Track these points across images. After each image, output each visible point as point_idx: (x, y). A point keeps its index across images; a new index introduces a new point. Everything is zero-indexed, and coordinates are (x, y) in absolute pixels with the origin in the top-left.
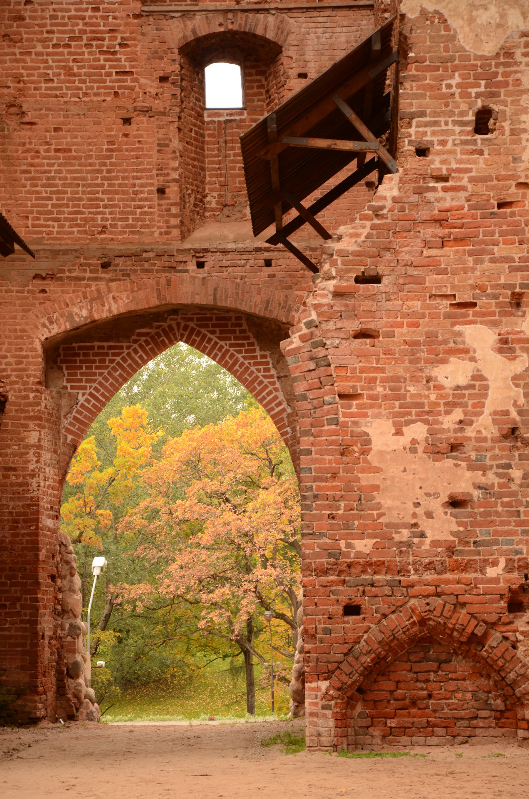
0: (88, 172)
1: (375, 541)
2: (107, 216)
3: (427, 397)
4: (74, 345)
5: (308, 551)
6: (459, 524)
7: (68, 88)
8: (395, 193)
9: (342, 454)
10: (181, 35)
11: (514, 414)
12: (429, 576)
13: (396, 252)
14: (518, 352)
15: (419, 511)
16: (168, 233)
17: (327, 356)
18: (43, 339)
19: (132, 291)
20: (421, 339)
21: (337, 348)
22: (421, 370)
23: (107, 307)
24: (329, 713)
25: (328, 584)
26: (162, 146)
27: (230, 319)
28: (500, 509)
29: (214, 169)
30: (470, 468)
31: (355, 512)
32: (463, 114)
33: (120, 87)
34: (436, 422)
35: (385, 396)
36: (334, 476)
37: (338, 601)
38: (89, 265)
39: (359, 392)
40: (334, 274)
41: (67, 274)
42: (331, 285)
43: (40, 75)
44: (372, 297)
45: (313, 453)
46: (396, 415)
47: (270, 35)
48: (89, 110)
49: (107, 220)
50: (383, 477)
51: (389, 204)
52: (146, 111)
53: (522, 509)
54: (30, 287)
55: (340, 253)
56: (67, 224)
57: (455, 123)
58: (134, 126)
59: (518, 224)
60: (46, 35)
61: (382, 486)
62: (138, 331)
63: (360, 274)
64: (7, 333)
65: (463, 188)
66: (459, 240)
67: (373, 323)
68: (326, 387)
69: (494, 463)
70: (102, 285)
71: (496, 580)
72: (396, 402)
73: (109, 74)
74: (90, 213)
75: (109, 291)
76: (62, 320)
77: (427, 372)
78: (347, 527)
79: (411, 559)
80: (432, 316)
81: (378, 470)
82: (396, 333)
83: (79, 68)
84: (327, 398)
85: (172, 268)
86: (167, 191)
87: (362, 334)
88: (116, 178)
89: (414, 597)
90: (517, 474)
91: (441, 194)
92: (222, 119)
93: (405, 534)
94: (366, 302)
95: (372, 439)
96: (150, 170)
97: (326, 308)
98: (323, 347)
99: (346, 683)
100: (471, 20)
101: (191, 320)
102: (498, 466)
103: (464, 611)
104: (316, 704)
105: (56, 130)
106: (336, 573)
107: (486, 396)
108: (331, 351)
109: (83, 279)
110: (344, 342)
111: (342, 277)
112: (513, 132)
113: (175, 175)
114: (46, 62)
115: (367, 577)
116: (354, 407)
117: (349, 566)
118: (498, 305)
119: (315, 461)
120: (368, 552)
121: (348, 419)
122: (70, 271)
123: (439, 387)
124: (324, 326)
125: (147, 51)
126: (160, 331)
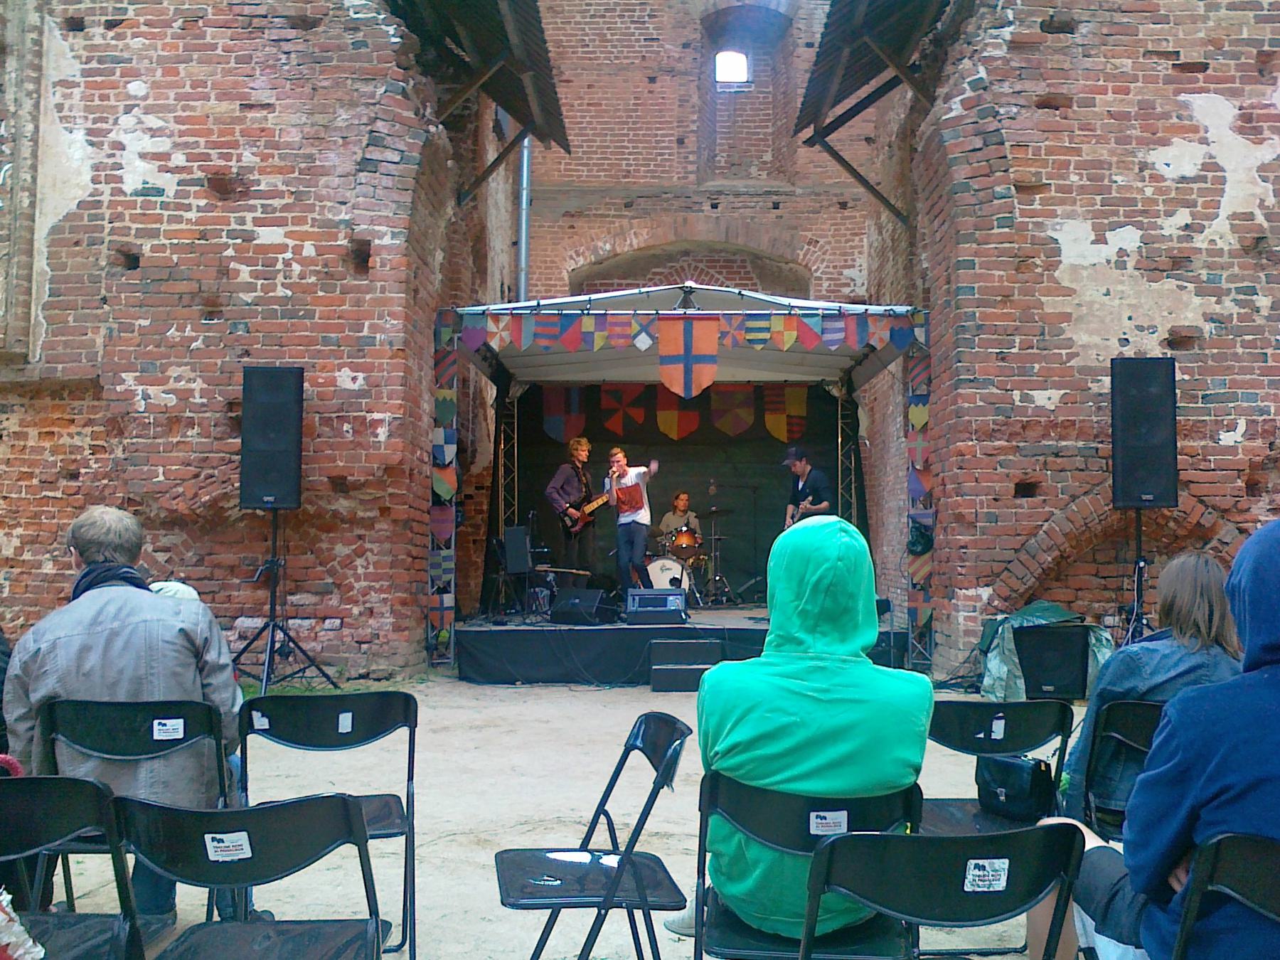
0: (616, 123)
1: (1062, 392)
2: (631, 162)
3: (1141, 191)
4: (598, 282)
5: (966, 405)
7: (601, 52)
10: (703, 8)
11: (1260, 219)
14: (1267, 133)
16: (686, 178)
17: (998, 130)
18: (570, 269)
19: (652, 228)
20: (1133, 110)
21: (1014, 119)
22: (1133, 154)
23: (628, 242)
25: (995, 452)
26: (683, 101)
27: (735, 261)
28: (1240, 350)
29: (725, 133)
31: (1035, 351)
33: (647, 52)
35: (1082, 187)
36: (1007, 297)
37: (1008, 476)
38: (614, 204)
39: (1045, 181)
40: (1011, 17)
41: (594, 212)
42: (1007, 32)
43: (578, 41)
44: (1063, 51)
45: (977, 266)
46: (1096, 215)
48: (619, 70)
49: (631, 165)
50: (1077, 302)
52: (671, 72)
53: (1269, 351)
54: (560, 223)
56: (595, 168)
58: (658, 84)
60: (584, 7)
61: (1074, 316)
62: (654, 270)
63: (1048, 18)
64: (539, 264)
67: (1065, 86)
68: (998, 174)
69: (1232, 286)
70: (625, 222)
71: (1232, 450)
72: (1096, 197)
73: (637, 41)
74: (616, 159)
75: (631, 228)
76: (587, 254)
80: (1147, 79)
81: (1070, 292)
82: (1097, 100)
83: (612, 35)
84: (998, 189)
86: (686, 141)
87: (1046, 103)
88: (640, 129)
90: (1263, 302)
92: (732, 90)
94: (1056, 57)
95: (1063, 248)
96: (670, 122)
97: (999, 62)
98: (994, 117)
99: (1016, 591)
101: (701, 261)
102: (1239, 290)
104: (973, 619)
105: (589, 87)
106: (1006, 437)
108: (1006, 123)
109: (608, 216)
110: (1023, 111)
111: (1022, 22)
114: (583, 29)
115: (1050, 443)
116: (1038, 202)
118: (1239, 67)
119: (980, 277)
120: (1053, 408)
121: (1028, 220)
122: (596, 209)
124: (996, 88)
125: (673, 21)
126: (673, 271)
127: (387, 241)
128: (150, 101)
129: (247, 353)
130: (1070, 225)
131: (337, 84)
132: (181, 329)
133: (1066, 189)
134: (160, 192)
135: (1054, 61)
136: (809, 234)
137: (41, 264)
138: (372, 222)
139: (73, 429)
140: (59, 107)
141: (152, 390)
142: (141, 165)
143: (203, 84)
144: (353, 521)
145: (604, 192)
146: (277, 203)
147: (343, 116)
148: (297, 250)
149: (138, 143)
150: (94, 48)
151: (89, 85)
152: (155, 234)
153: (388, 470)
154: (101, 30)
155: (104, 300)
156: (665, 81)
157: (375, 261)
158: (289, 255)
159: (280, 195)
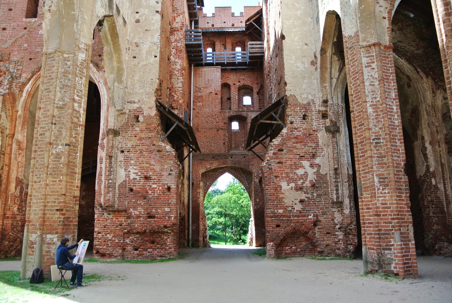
3: (294, 177)
6: (302, 206)
8: (286, 132)
9: (275, 190)
11: (314, 181)
12: (295, 218)
13: (287, 145)
14: (315, 167)
15: (293, 203)
20: (293, 164)
22: (293, 171)
24: (273, 250)
26: (224, 135)
28: (311, 203)
30: (305, 193)
32: (300, 115)
34: (297, 183)
36: (274, 194)
42: (272, 151)
44: (282, 154)
46: (287, 181)
47: (245, 116)
51: (285, 134)
52: (222, 129)
53: (316, 203)
55: (274, 144)
57: (298, 117)
59: (313, 139)
65: (301, 131)
66: (300, 142)
70: (213, 161)
71: (311, 219)
77: (294, 171)
78: (277, 207)
79: (292, 214)
80: (295, 159)
81: (284, 194)
84: (272, 177)
85: (226, 158)
87: (279, 163)
90: (315, 195)
91: (296, 132)
93: (290, 208)
100: (301, 97)
102: (311, 193)
107: (308, 177)
108: (273, 166)
112: (311, 120)
117: (277, 216)
118: (310, 156)
119: (269, 191)
123: (297, 175)
124: (271, 161)
127: (173, 187)
128: (135, 164)
129: (151, 205)
130: (283, 183)
131: (165, 161)
132: (140, 201)
133: (283, 177)
134: (136, 179)
135: (280, 156)
136: (252, 163)
137: (117, 191)
138: (171, 184)
139: (121, 218)
140: (120, 165)
141: (135, 211)
143: (143, 161)
144: (167, 233)
145: (208, 155)
146: (155, 181)
148: (159, 188)
149: (132, 171)
150: (125, 155)
152: (136, 186)
153: (174, 224)
154: (127, 152)
155: (127, 197)
156: (221, 131)
157: (171, 190)
158: (157, 189)
159: (156, 179)
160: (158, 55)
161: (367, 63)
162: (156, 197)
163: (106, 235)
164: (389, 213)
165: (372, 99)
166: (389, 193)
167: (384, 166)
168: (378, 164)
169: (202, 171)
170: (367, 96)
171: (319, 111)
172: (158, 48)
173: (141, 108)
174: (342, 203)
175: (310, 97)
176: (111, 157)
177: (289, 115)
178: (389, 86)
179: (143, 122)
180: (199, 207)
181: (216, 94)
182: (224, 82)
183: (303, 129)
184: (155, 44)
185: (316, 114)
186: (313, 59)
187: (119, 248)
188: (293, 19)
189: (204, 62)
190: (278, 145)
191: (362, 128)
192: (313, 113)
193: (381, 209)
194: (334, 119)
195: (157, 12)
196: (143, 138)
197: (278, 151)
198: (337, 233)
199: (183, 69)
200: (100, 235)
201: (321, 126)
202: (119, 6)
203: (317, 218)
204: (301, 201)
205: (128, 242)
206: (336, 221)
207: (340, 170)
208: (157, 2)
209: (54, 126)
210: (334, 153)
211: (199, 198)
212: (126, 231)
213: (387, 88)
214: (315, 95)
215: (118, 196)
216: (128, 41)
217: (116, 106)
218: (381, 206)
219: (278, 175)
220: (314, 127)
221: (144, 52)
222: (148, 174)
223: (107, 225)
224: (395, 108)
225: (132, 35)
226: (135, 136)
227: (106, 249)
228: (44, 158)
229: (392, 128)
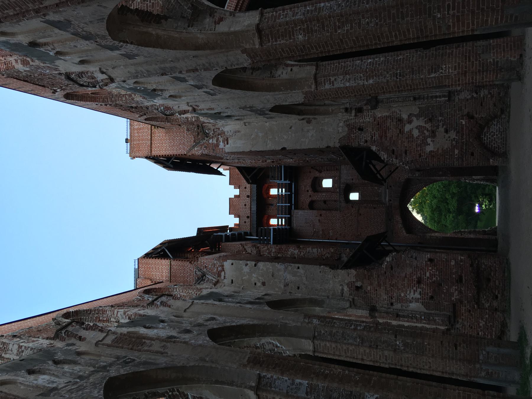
3: (421, 138)
6: (452, 130)
8: (375, 147)
11: (426, 119)
12: (465, 137)
14: (411, 119)
15: (448, 139)
20: (407, 140)
24: (498, 159)
30: (438, 128)
32: (359, 134)
47: (345, 186)
51: (377, 148)
55: (387, 158)
57: (361, 135)
65: (375, 133)
66: (386, 133)
69: (437, 123)
71: (466, 122)
76: (402, 230)
79: (460, 141)
81: (438, 149)
87: (406, 153)
89: (469, 140)
90: (440, 118)
100: (341, 133)
102: (438, 122)
103: (473, 129)
105: (362, 229)
107: (421, 126)
113: (372, 205)
117: (461, 155)
118: (400, 124)
123: (419, 136)
127: (429, 256)
128: (405, 293)
129: (448, 279)
134: (420, 292)
137: (433, 312)
138: (425, 258)
139: (461, 310)
140: (406, 307)
141: (455, 295)
142: (416, 295)
143: (402, 284)
147: (408, 262)
148: (430, 270)
149: (412, 295)
151: (402, 303)
152: (428, 293)
154: (393, 300)
155: (439, 302)
157: (432, 258)
158: (431, 272)
159: (421, 273)
160: (297, 265)
161: (330, 84)
162: (439, 273)
163: (480, 327)
164: (464, 64)
165: (361, 80)
166: (445, 65)
167: (421, 68)
168: (419, 74)
169: (403, 233)
170: (358, 84)
171: (356, 116)
172: (290, 265)
173: (348, 283)
174: (450, 92)
175: (341, 124)
176: (398, 316)
177: (359, 144)
178: (350, 66)
179: (363, 282)
180: (448, 237)
181: (321, 215)
182: (307, 207)
183: (373, 131)
184: (286, 268)
185: (358, 119)
186: (305, 121)
187: (495, 314)
188: (266, 140)
189: (287, 227)
190: (387, 155)
191: (386, 88)
192: (357, 121)
193: (460, 71)
194: (365, 102)
195: (255, 265)
196: (378, 282)
197: (393, 154)
198: (482, 96)
199: (299, 247)
200: (480, 333)
201: (370, 114)
202: (256, 297)
203: (465, 115)
204: (446, 131)
205: (489, 304)
206: (470, 97)
207: (415, 95)
208: (246, 265)
209: (379, 347)
210: (398, 102)
211: (437, 237)
212: (476, 306)
213: (352, 68)
214: (339, 120)
215: (438, 312)
216: (282, 293)
217: (346, 307)
218: (457, 70)
219: (418, 154)
220: (370, 120)
221: (293, 278)
222: (416, 280)
223: (470, 326)
224: (370, 60)
225: (277, 290)
226: (376, 291)
227: (496, 328)
228: (408, 358)
229: (388, 63)
